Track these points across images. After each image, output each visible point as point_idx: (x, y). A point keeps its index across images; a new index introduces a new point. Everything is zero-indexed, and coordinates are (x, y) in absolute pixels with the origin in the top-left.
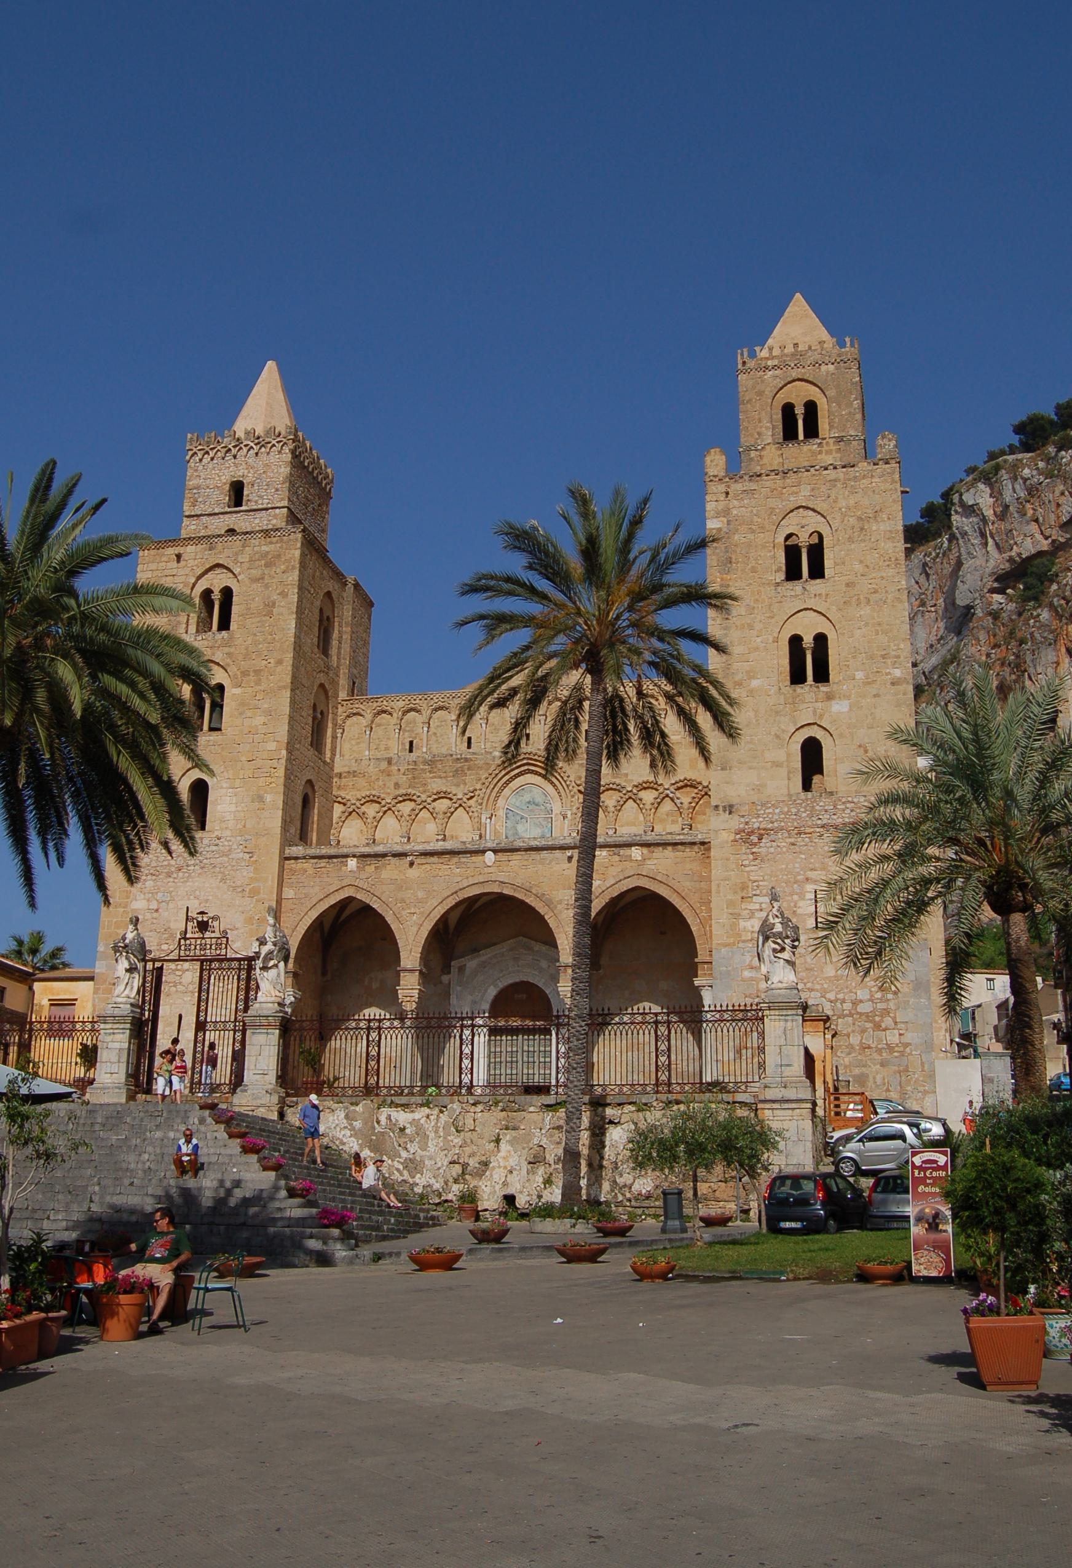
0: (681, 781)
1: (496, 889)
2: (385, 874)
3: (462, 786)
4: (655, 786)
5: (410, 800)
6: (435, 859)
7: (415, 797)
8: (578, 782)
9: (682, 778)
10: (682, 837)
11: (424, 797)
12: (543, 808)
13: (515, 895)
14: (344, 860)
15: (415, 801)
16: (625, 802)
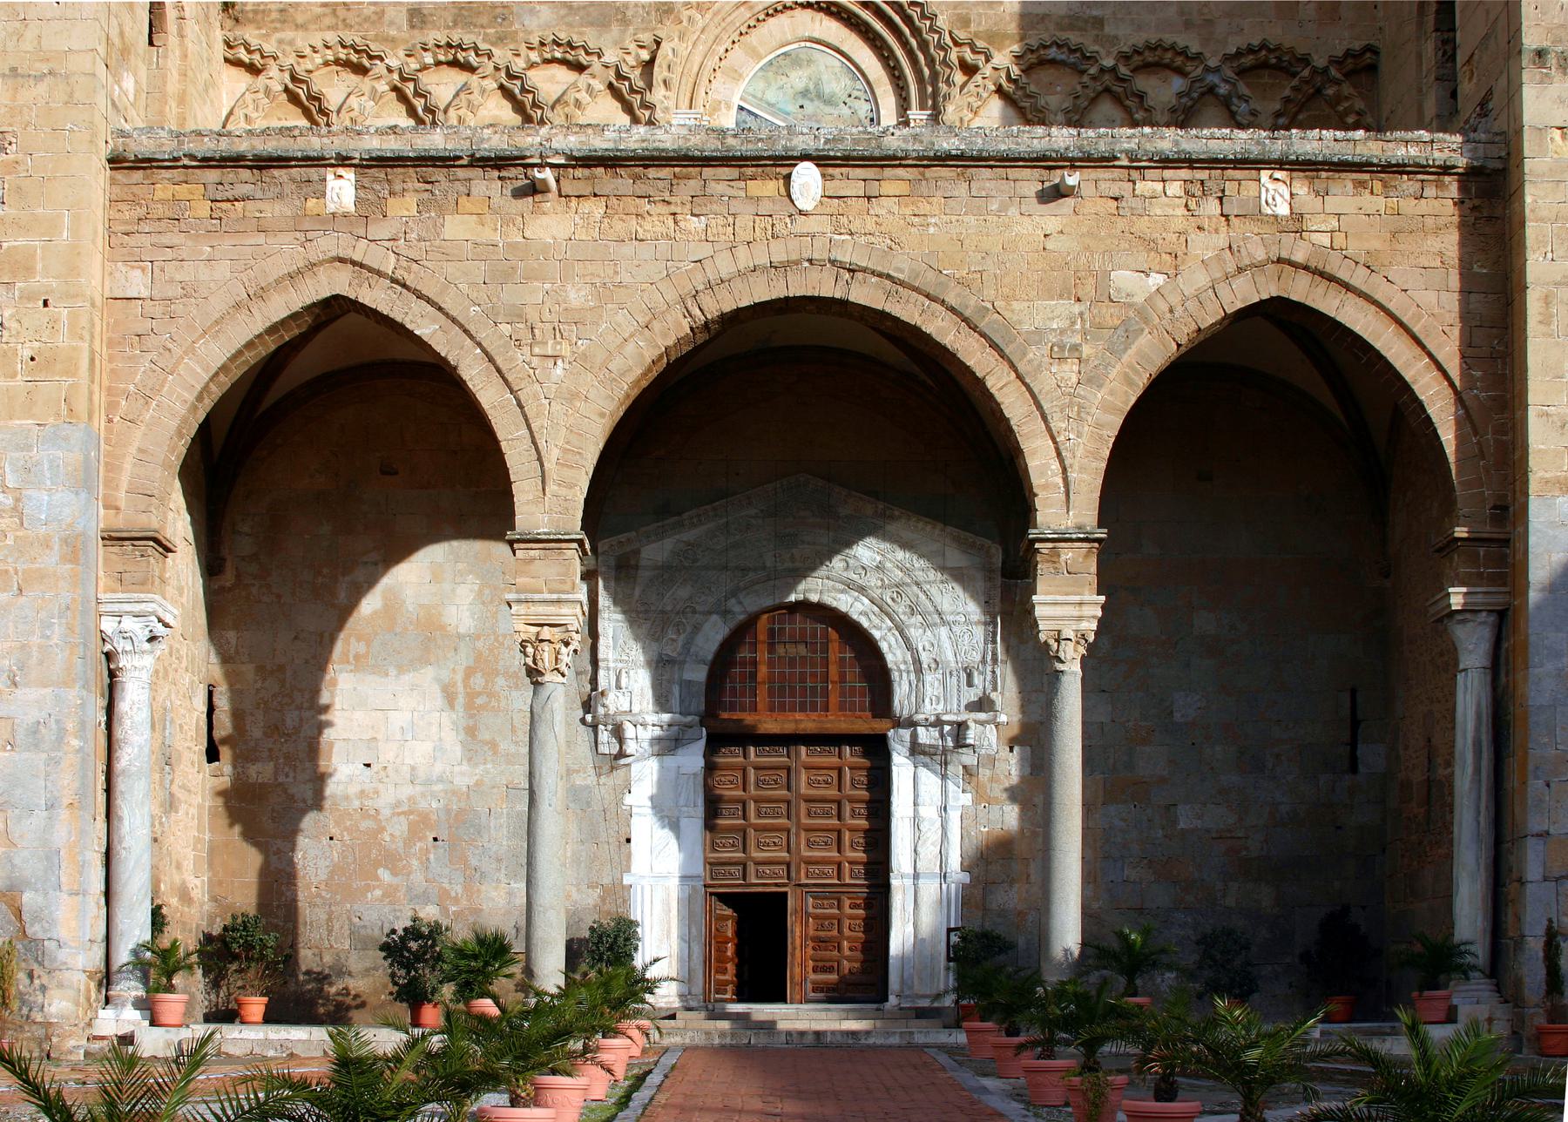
0: (1251, 50)
1: (825, 286)
2: (457, 227)
3: (615, 29)
4: (1179, 61)
5: (454, 63)
6: (623, 182)
7: (473, 59)
8: (961, 35)
9: (1256, 42)
10: (1413, 151)
11: (501, 55)
12: (846, 111)
13: (887, 310)
14: (313, 173)
15: (469, 68)
16: (1093, 101)
